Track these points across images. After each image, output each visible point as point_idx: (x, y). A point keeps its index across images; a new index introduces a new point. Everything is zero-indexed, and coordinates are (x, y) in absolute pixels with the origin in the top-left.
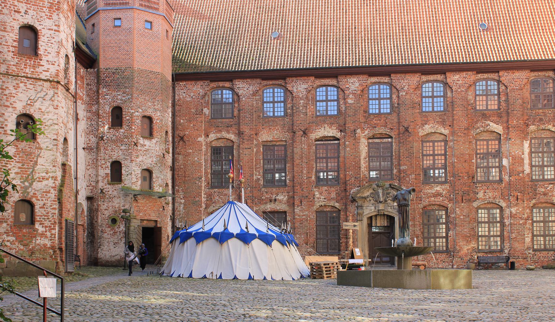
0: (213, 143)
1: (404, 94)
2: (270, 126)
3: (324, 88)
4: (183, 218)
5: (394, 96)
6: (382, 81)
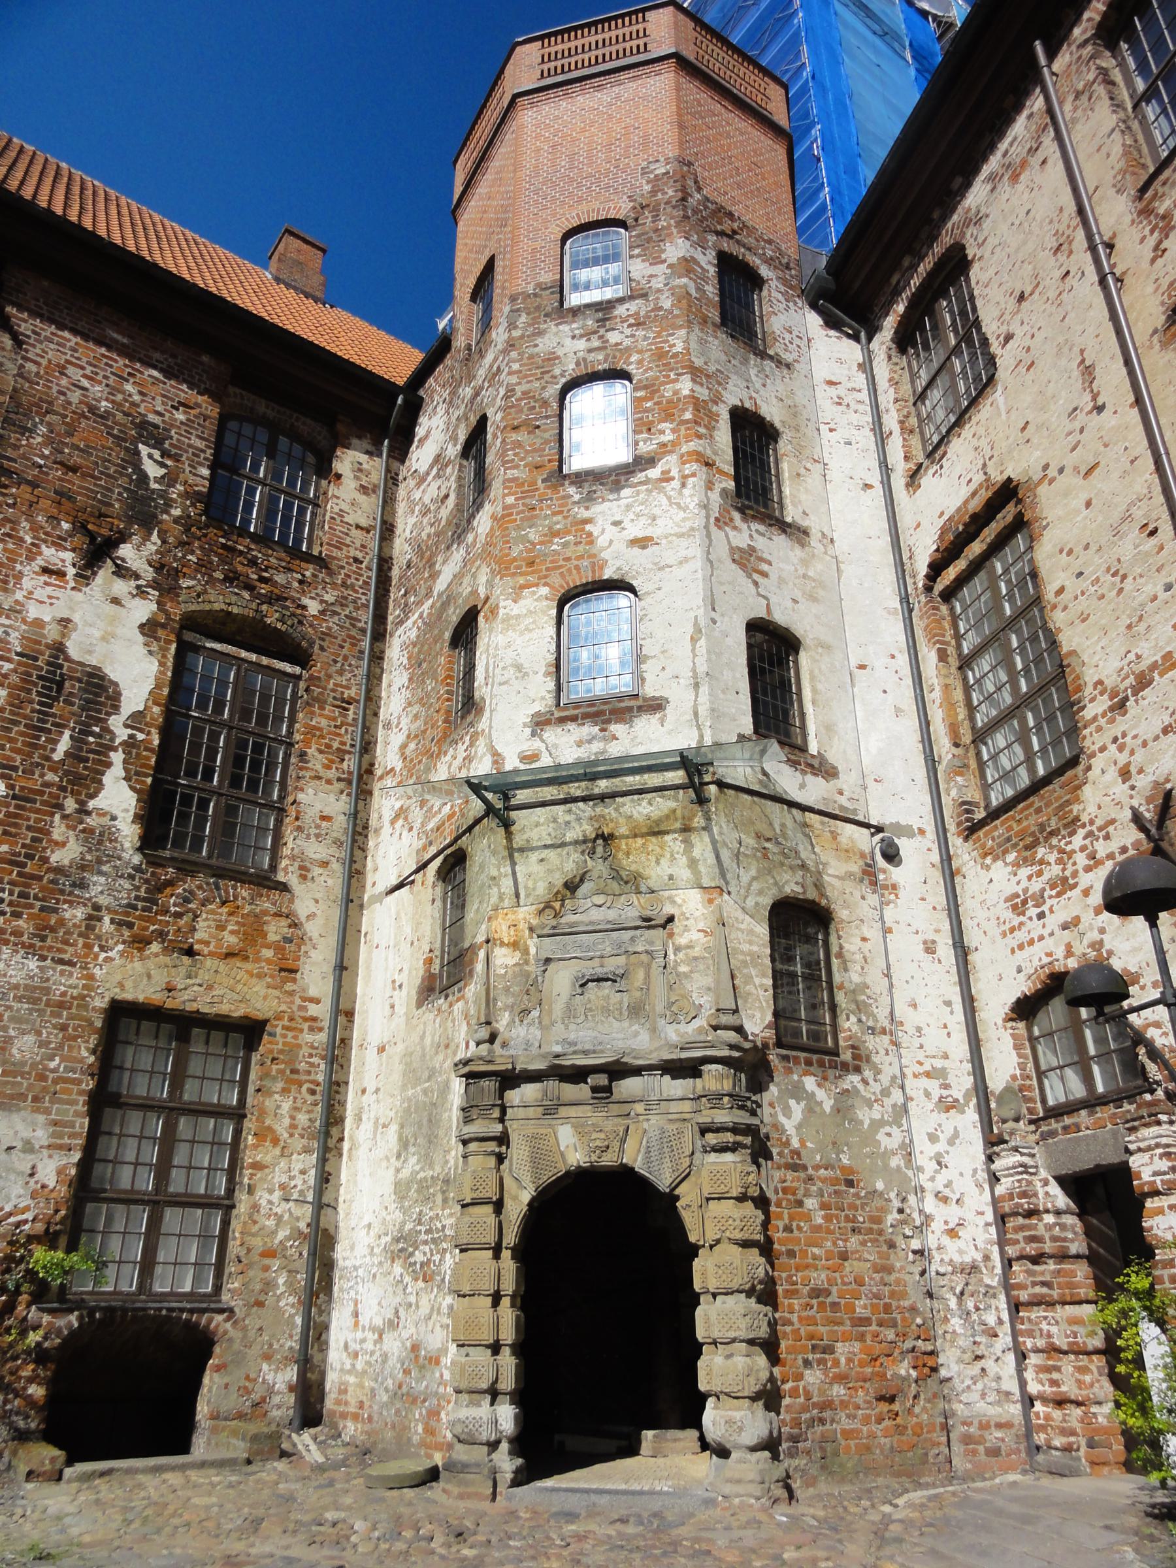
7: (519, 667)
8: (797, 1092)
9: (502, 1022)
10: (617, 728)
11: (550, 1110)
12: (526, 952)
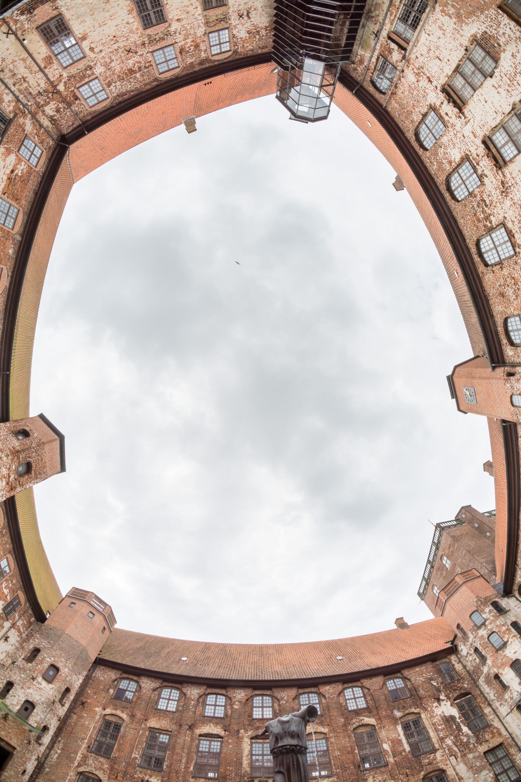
0: (107, 716)
1: (284, 702)
2: (160, 716)
3: (214, 696)
4: (52, 765)
5: (276, 705)
6: (265, 693)
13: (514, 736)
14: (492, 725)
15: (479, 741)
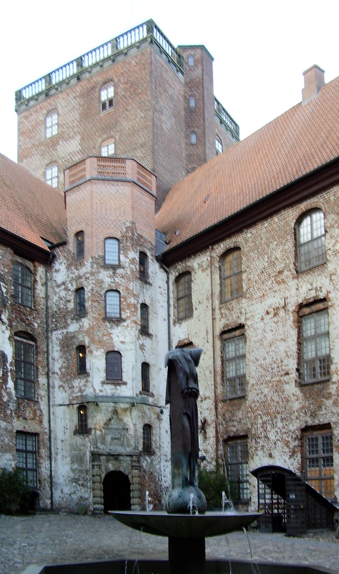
7: (98, 369)
8: (146, 460)
9: (99, 444)
10: (118, 387)
11: (108, 461)
12: (102, 432)
13: (52, 436)
14: (38, 402)
15: (19, 413)
